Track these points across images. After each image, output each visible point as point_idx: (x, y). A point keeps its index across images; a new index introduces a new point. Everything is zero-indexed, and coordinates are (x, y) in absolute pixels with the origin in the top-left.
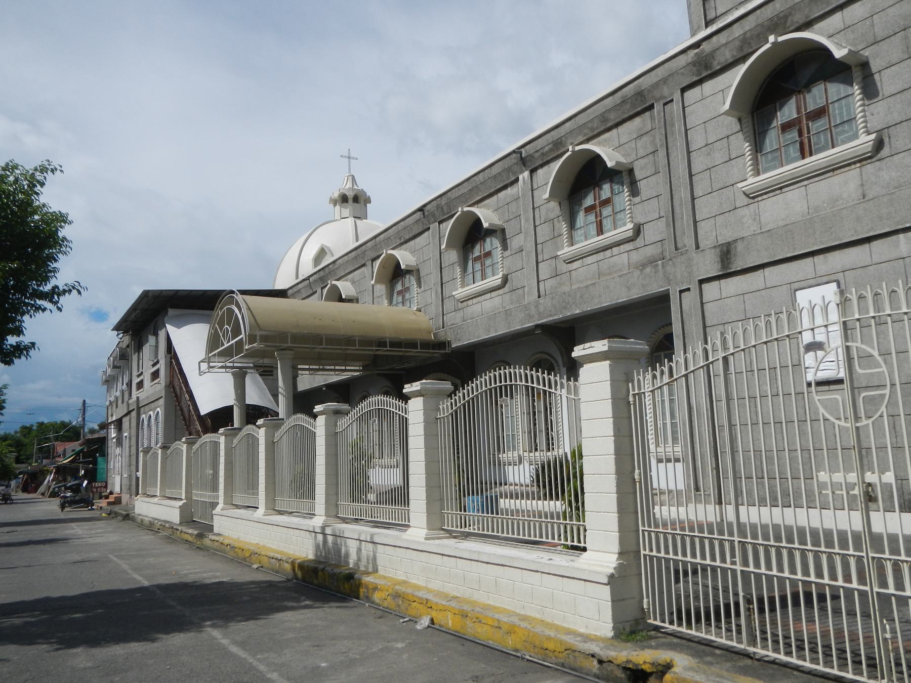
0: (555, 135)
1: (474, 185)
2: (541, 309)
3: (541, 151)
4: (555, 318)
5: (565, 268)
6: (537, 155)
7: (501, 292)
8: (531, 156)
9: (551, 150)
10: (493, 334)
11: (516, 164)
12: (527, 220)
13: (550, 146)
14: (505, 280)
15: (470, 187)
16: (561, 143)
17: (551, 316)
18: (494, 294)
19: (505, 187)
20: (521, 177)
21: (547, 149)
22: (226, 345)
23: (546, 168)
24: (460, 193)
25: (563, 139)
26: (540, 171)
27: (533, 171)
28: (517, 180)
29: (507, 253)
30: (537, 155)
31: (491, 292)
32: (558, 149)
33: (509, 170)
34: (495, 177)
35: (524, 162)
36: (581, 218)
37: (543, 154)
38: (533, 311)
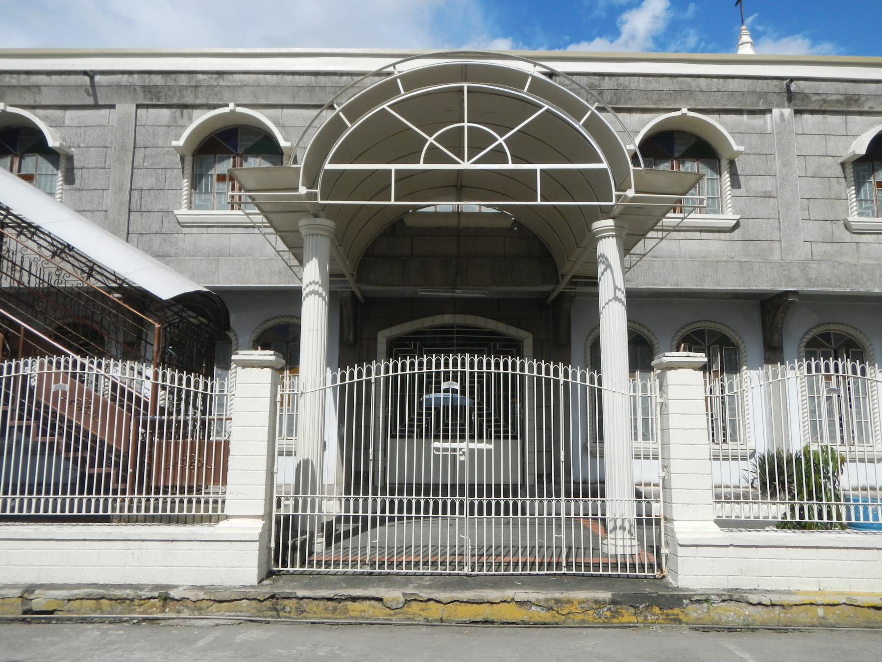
0: (852, 89)
1: (685, 87)
2: (813, 274)
3: (824, 97)
4: (837, 289)
5: (848, 236)
6: (814, 98)
7: (723, 236)
8: (805, 96)
9: (838, 101)
10: (708, 285)
11: (779, 94)
12: (785, 164)
13: (839, 97)
14: (737, 226)
15: (677, 88)
16: (857, 101)
17: (831, 286)
18: (705, 235)
19: (739, 112)
20: (776, 111)
21: (833, 97)
22: (466, 165)
23: (819, 117)
24: (650, 87)
25: (863, 98)
26: (807, 117)
27: (797, 112)
28: (770, 111)
29: (737, 192)
30: (814, 98)
31: (701, 231)
32: (849, 104)
33: (763, 95)
34: (732, 93)
35: (790, 96)
36: (869, 189)
37: (825, 101)
38: (796, 273)
